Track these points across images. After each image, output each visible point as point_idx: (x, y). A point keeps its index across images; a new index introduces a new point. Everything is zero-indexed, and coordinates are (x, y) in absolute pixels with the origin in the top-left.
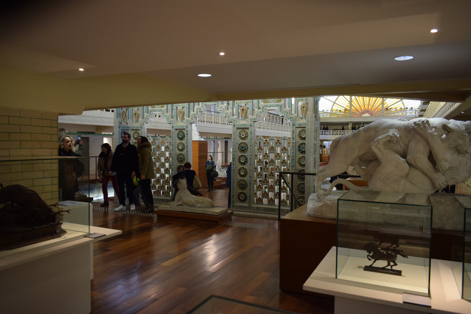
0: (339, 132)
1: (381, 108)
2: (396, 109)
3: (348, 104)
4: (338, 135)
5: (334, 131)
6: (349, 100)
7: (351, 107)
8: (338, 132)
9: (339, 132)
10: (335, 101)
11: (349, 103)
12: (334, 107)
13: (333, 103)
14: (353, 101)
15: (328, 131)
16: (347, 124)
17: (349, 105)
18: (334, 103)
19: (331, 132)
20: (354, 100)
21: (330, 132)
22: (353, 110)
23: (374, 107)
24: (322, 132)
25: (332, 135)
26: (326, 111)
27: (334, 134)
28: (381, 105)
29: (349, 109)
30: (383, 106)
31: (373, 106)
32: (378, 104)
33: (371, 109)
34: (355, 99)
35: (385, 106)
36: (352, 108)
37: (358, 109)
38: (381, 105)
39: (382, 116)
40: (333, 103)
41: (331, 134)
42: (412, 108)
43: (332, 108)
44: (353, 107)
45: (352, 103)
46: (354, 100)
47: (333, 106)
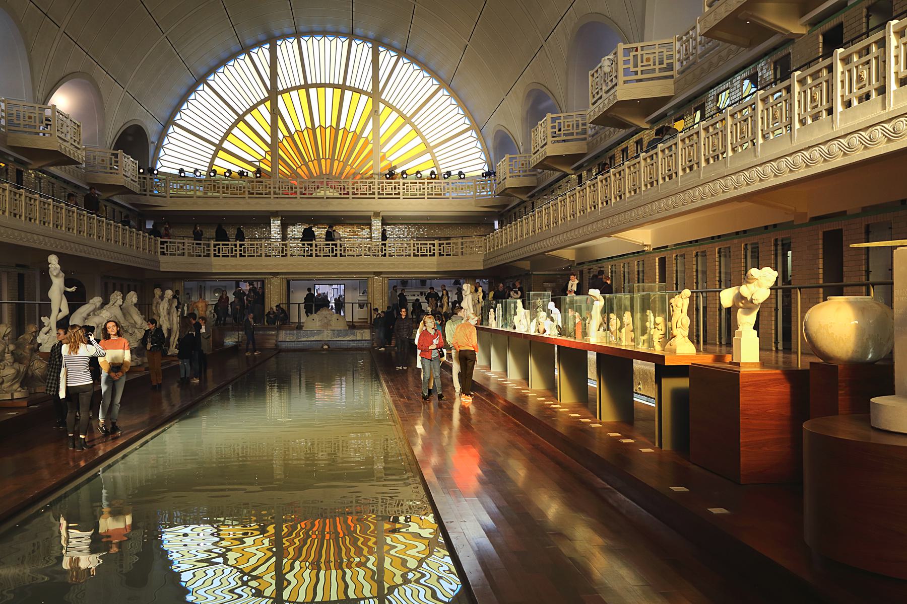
0: (238, 248)
2: (419, 176)
3: (266, 152)
4: (235, 256)
5: (221, 243)
6: (269, 140)
7: (274, 164)
8: (236, 247)
9: (238, 248)
12: (217, 161)
14: (280, 145)
15: (202, 242)
16: (262, 220)
17: (269, 158)
18: (219, 147)
19: (212, 248)
20: (285, 142)
21: (208, 246)
23: (348, 168)
24: (181, 246)
25: (215, 255)
26: (191, 175)
27: (221, 254)
29: (269, 169)
33: (341, 173)
37: (299, 170)
39: (379, 194)
41: (212, 253)
42: (460, 173)
43: (212, 163)
44: (284, 165)
45: (280, 152)
46: (285, 142)
47: (213, 159)
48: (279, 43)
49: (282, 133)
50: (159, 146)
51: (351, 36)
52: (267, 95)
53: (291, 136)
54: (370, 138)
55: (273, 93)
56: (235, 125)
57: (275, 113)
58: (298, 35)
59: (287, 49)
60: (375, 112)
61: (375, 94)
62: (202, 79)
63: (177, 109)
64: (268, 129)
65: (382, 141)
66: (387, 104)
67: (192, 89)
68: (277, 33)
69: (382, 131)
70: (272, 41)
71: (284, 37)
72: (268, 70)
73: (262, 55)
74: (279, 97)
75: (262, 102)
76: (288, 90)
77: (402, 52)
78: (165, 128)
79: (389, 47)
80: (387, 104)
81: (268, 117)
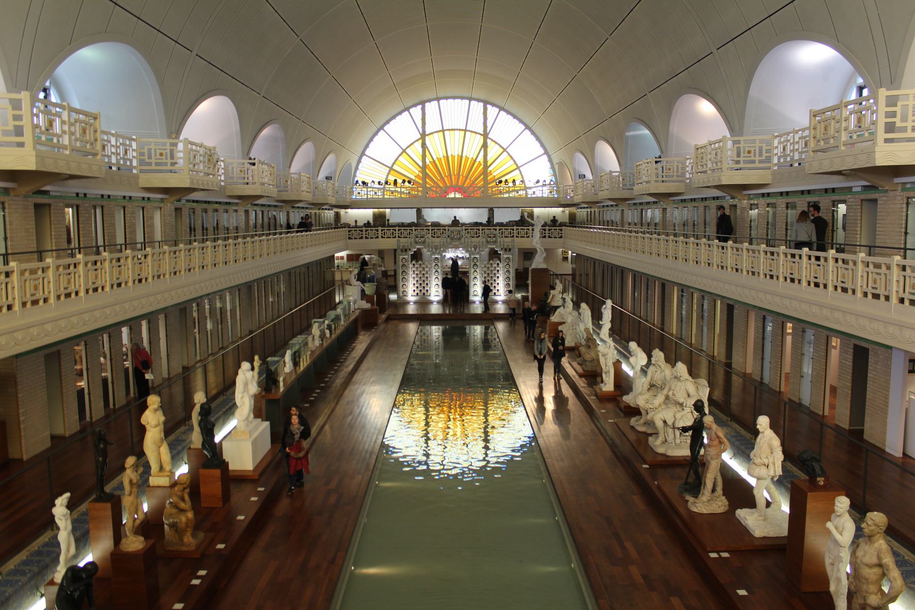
1: (482, 183)
6: (421, 164)
7: (424, 179)
10: (393, 165)
11: (420, 170)
13: (388, 169)
17: (421, 175)
18: (391, 169)
22: (429, 184)
28: (482, 176)
29: (421, 182)
30: (485, 179)
31: (467, 178)
32: (475, 175)
34: (433, 163)
35: (489, 178)
36: (427, 180)
38: (482, 176)
40: (388, 169)
45: (427, 171)
47: (387, 176)
48: (427, 104)
49: (428, 160)
50: (357, 168)
51: (470, 99)
52: (420, 137)
53: (434, 161)
54: (482, 162)
55: (423, 135)
56: (401, 155)
57: (424, 146)
58: (438, 99)
59: (431, 107)
60: (485, 146)
61: (485, 135)
62: (382, 128)
63: (367, 146)
64: (421, 158)
65: (489, 164)
66: (492, 140)
67: (376, 134)
68: (425, 98)
69: (489, 157)
70: (423, 103)
71: (430, 101)
72: (421, 121)
73: (416, 111)
74: (427, 137)
75: (417, 141)
76: (432, 133)
77: (501, 109)
78: (360, 158)
79: (493, 105)
80: (492, 140)
81: (420, 150)
